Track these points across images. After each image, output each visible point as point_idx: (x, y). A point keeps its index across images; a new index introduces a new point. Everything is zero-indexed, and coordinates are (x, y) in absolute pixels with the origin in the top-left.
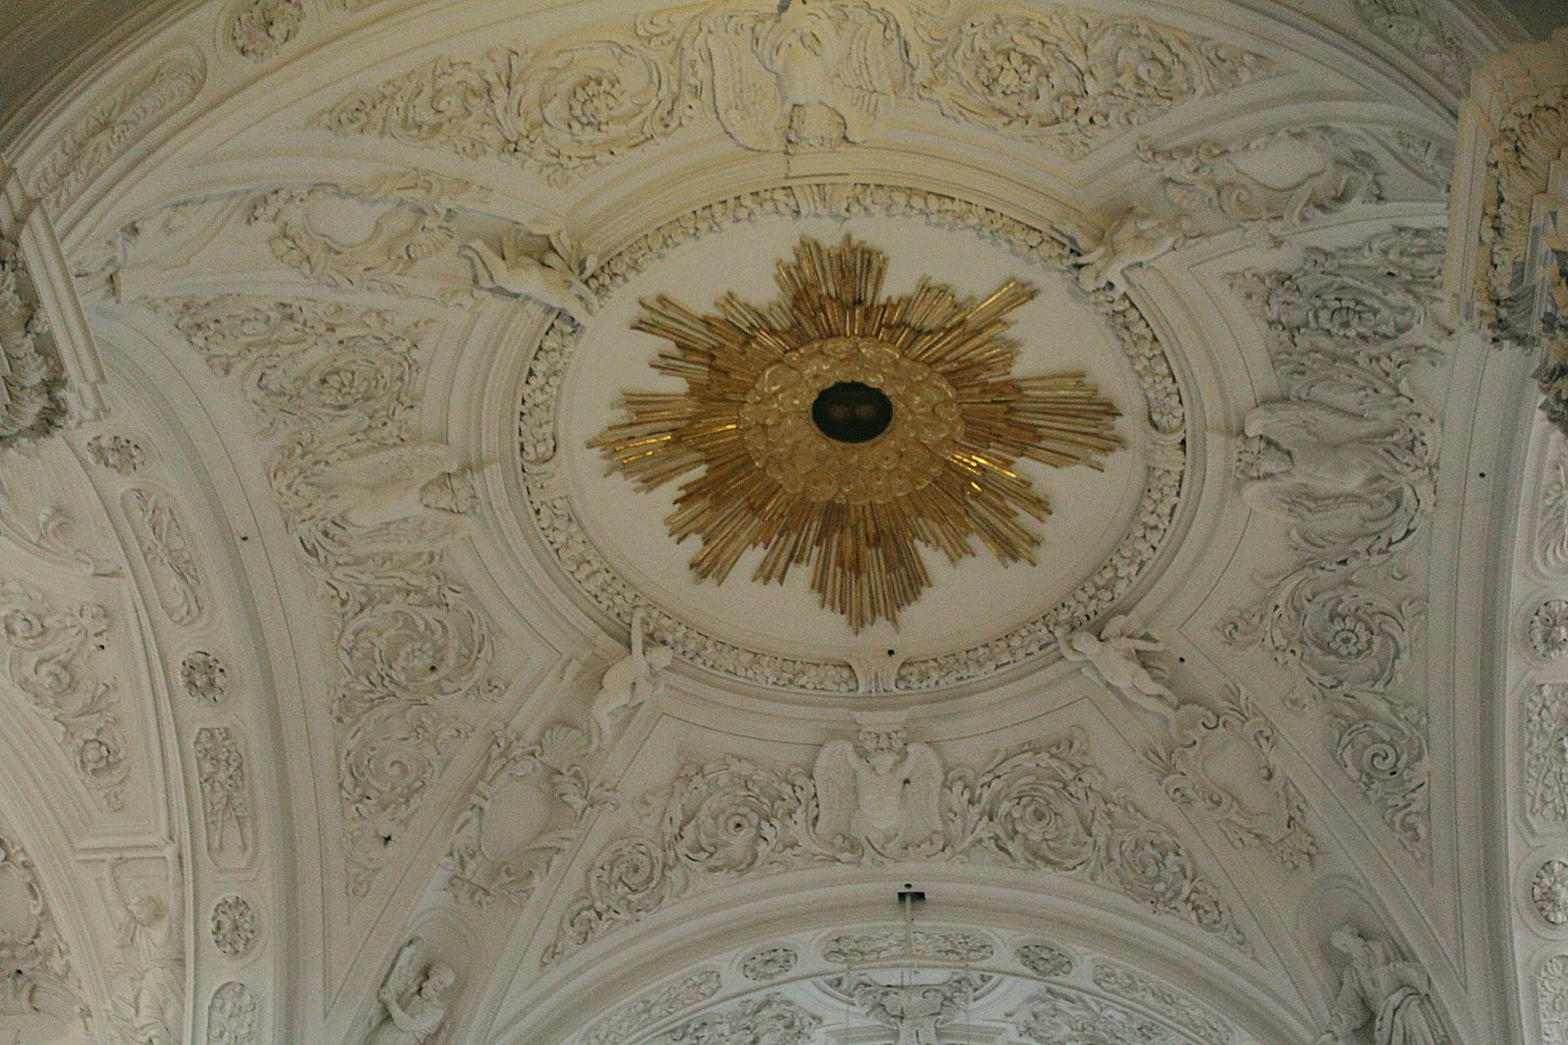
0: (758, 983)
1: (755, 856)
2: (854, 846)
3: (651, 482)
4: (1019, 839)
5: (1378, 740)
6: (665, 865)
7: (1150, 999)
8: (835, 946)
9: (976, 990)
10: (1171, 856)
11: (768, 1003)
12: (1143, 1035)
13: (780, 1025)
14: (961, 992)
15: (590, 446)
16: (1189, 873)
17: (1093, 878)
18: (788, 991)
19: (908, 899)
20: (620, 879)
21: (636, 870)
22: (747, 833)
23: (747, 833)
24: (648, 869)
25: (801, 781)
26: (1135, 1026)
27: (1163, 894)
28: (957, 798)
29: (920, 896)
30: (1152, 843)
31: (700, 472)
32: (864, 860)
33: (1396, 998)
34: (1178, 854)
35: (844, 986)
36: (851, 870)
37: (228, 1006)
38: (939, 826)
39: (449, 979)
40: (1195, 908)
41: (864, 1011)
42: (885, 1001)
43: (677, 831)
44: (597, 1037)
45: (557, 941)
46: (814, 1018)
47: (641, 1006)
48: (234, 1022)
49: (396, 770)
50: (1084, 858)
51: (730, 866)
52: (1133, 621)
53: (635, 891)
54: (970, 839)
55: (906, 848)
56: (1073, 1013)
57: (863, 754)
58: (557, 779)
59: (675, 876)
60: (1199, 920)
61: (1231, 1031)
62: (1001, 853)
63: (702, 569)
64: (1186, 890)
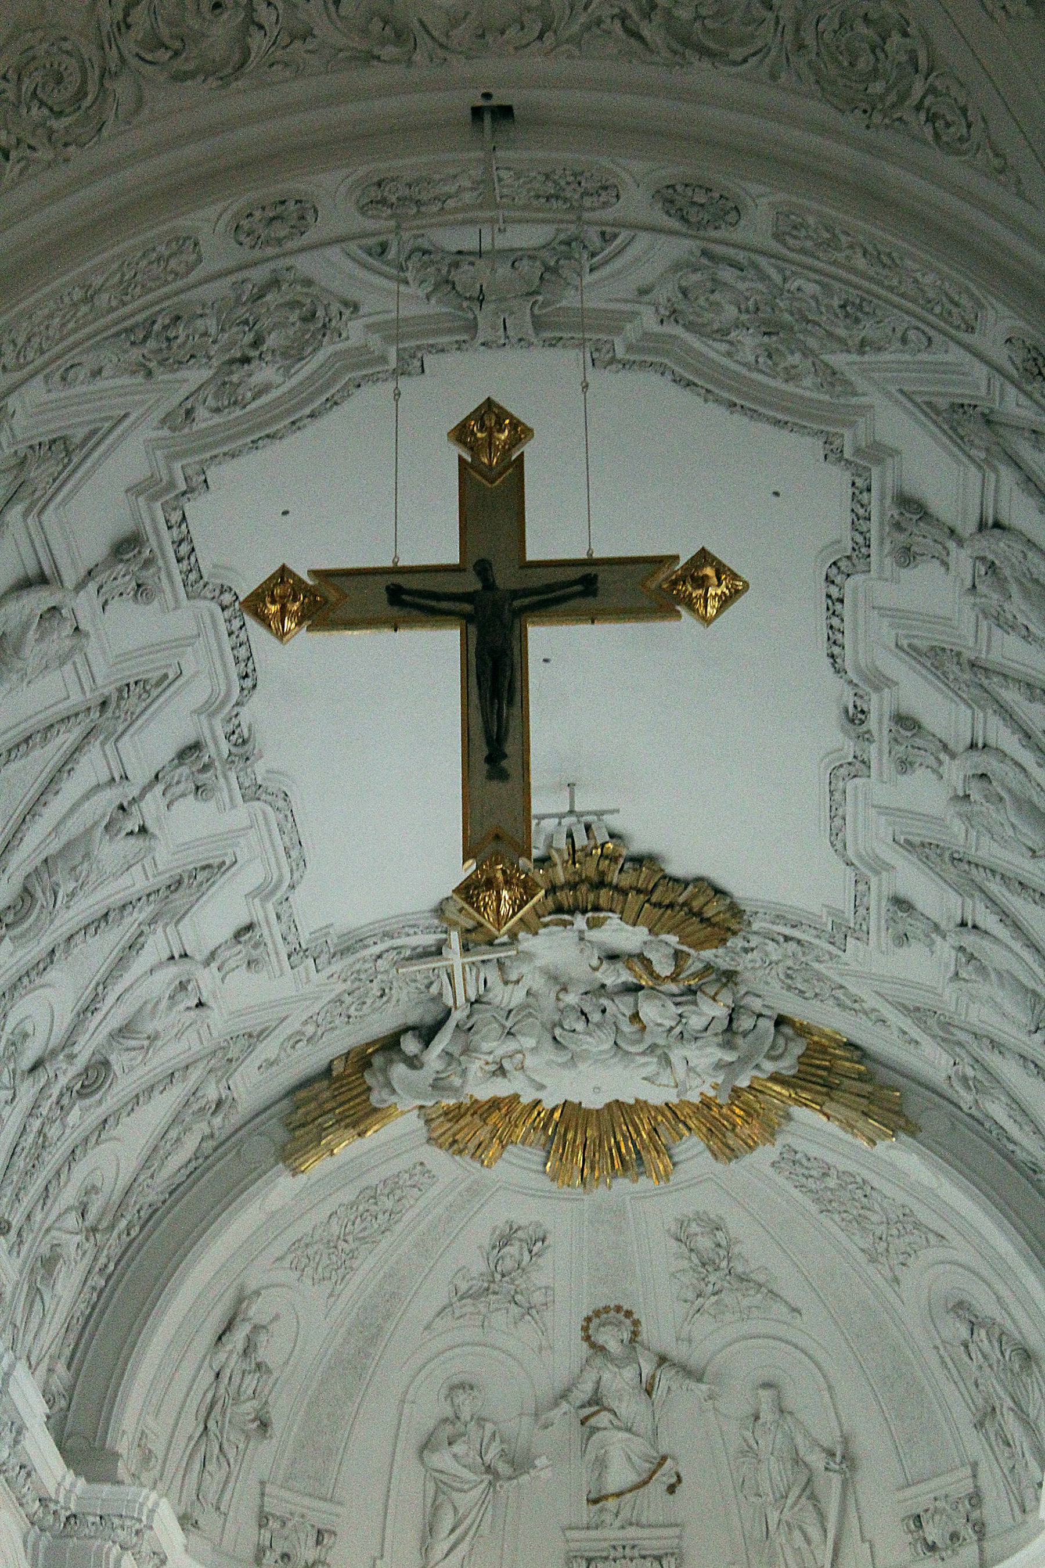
0: (257, 253)
1: (246, 53)
2: (400, 36)
4: (657, 17)
6: (104, 72)
7: (861, 263)
8: (374, 193)
9: (593, 255)
10: (896, 38)
11: (275, 283)
12: (847, 316)
13: (294, 316)
14: (569, 258)
17: (774, 77)
18: (305, 264)
19: (487, 118)
20: (34, 93)
21: (59, 80)
22: (230, 20)
24: (77, 78)
26: (836, 303)
27: (882, 98)
29: (505, 112)
32: (417, 57)
34: (905, 34)
35: (391, 254)
40: (932, 118)
41: (421, 293)
42: (456, 276)
43: (120, 16)
44: (14, 342)
46: (346, 304)
47: (78, 294)
50: (760, 44)
51: (204, 72)
53: (59, 114)
54: (583, 19)
55: (482, 36)
56: (742, 286)
59: (122, 88)
60: (937, 136)
61: (982, 307)
62: (632, 41)
64: (918, 88)
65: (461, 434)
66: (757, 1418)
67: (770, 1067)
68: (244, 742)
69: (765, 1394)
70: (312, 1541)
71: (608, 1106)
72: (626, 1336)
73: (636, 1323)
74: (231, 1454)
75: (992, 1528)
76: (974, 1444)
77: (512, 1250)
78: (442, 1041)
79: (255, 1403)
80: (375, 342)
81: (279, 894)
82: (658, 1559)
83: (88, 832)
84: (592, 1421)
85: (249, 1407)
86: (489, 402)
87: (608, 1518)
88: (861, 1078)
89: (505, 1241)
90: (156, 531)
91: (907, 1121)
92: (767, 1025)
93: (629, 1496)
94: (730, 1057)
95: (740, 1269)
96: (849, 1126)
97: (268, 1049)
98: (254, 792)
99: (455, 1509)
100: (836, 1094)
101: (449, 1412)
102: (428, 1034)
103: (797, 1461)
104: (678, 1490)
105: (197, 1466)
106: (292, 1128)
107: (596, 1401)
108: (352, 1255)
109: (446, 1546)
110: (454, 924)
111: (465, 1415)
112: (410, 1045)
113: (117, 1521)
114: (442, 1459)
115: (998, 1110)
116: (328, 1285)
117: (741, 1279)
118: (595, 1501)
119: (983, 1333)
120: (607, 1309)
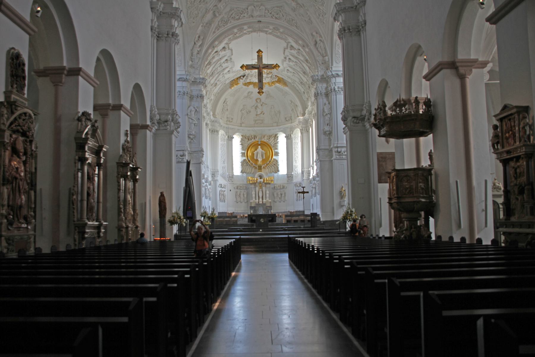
2: (252, 16)
5: (321, 12)
23: (239, 16)
25: (246, 10)
28: (267, 12)
29: (260, 21)
33: (319, 42)
38: (264, 14)
39: (202, 38)
51: (237, 19)
57: (254, 7)
59: (229, 22)
65: (257, 52)
66: (271, 108)
67: (275, 80)
69: (272, 106)
72: (260, 100)
77: (250, 93)
78: (245, 77)
80: (247, 32)
85: (226, 109)
88: (283, 81)
89: (249, 93)
92: (274, 76)
97: (229, 79)
98: (231, 62)
102: (244, 76)
103: (275, 112)
106: (231, 85)
107: (257, 106)
112: (242, 77)
114: (243, 112)
115: (295, 85)
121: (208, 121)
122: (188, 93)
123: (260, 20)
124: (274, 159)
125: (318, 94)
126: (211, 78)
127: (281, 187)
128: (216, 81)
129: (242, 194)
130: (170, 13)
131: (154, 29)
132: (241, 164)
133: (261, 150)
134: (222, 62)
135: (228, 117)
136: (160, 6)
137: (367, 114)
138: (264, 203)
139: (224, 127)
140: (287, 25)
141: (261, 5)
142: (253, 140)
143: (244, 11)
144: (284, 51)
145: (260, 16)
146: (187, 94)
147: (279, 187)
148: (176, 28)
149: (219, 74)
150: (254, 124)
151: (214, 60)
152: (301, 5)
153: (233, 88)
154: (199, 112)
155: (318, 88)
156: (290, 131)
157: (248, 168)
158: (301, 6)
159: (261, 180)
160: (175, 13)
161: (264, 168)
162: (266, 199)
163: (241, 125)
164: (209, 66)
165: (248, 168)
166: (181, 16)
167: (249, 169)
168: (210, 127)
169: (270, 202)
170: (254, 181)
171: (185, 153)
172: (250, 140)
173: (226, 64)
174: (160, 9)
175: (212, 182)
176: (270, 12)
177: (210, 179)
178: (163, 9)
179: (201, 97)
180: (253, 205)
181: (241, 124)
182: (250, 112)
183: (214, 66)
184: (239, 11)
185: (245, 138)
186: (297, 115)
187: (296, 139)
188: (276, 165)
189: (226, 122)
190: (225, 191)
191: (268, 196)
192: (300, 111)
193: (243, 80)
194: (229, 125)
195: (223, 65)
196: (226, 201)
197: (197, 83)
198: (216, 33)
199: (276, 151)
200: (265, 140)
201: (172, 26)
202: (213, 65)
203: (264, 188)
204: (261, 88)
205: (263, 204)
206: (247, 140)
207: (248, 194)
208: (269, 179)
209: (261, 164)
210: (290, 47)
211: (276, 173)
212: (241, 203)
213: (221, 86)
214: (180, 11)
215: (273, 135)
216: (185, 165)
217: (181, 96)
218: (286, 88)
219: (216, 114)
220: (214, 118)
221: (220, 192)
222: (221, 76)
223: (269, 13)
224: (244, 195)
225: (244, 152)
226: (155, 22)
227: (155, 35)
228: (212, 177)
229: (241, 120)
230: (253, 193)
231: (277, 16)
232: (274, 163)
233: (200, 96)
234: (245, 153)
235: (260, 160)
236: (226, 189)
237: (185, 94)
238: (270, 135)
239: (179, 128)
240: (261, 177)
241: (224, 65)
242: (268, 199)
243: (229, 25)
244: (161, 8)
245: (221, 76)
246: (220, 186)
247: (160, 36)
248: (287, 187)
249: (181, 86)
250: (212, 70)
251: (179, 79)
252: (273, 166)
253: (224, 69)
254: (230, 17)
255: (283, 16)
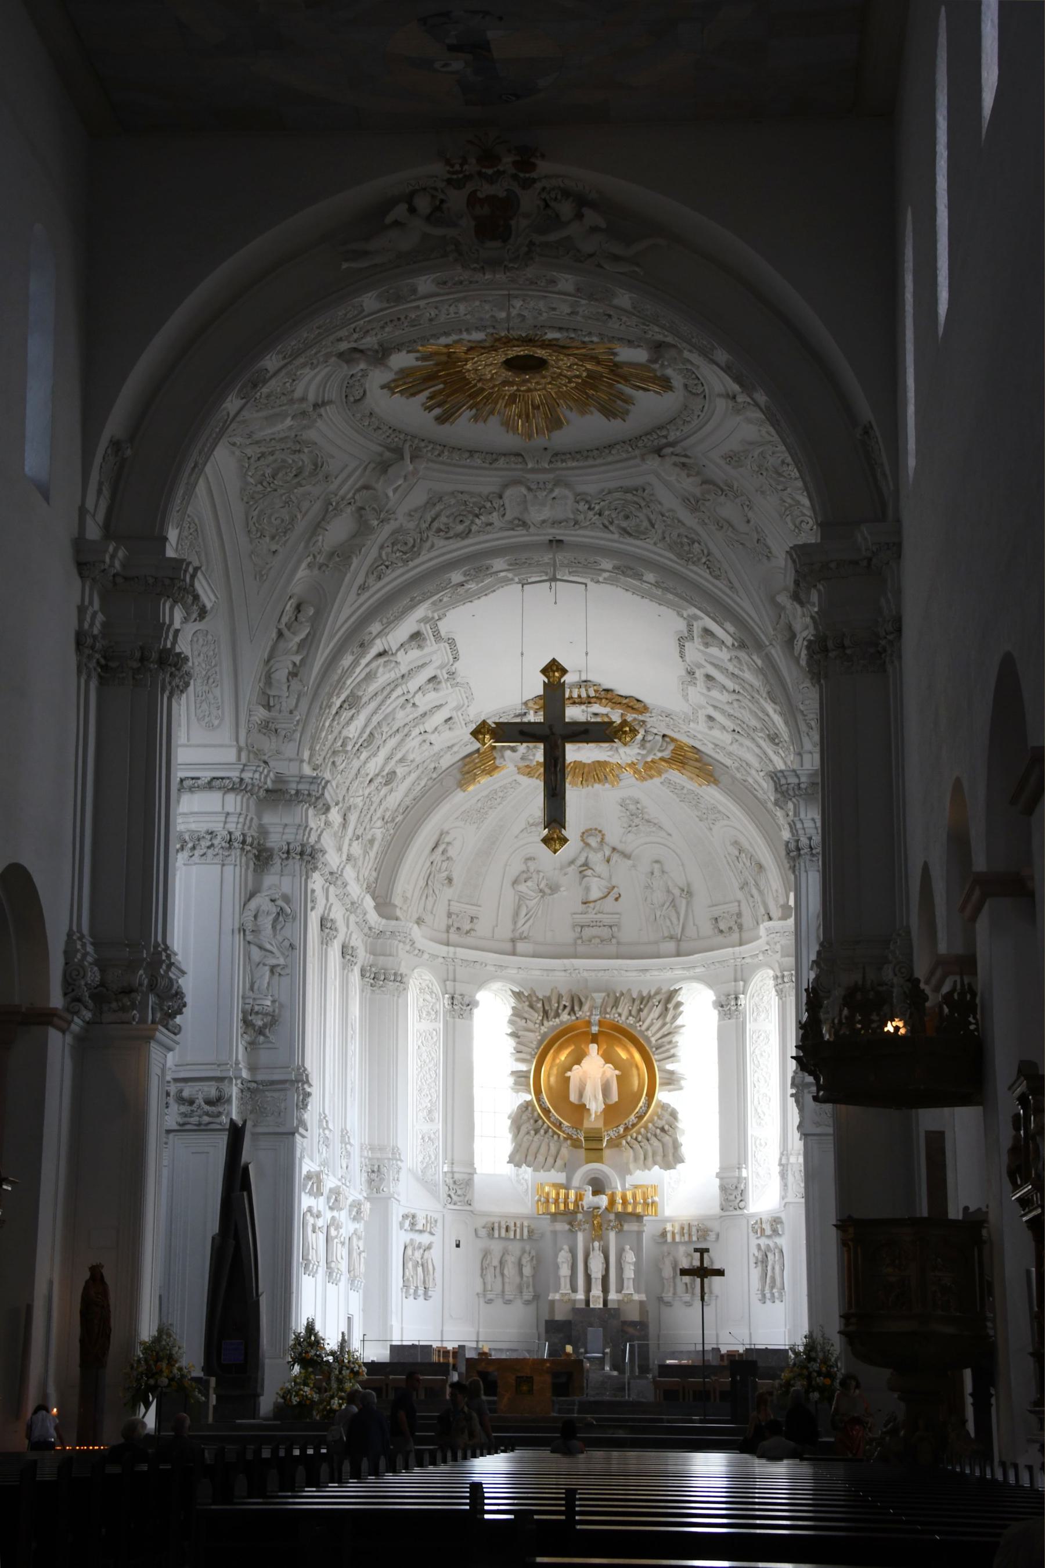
2: (524, 524)
3: (413, 395)
15: (383, 387)
16: (706, 552)
19: (554, 543)
23: (467, 523)
30: (686, 536)
31: (441, 386)
36: (524, 532)
37: (201, 640)
39: (311, 611)
45: (365, 582)
48: (205, 649)
49: (279, 521)
52: (678, 449)
57: (529, 489)
58: (363, 512)
59: (428, 544)
63: (441, 420)
65: (544, 671)
66: (652, 873)
67: (660, 755)
68: (453, 673)
69: (656, 866)
70: (469, 922)
71: (593, 762)
72: (599, 840)
73: (603, 835)
74: (437, 893)
75: (745, 927)
76: (740, 895)
79: (446, 873)
81: (463, 709)
82: (611, 927)
83: (395, 709)
84: (585, 873)
85: (445, 874)
86: (554, 661)
87: (590, 910)
88: (697, 760)
90: (426, 630)
91: (715, 780)
93: (599, 902)
94: (644, 752)
95: (646, 817)
96: (692, 779)
97: (455, 749)
99: (527, 907)
100: (686, 766)
101: (524, 868)
103: (669, 891)
104: (620, 900)
105: (424, 898)
107: (586, 864)
108: (486, 813)
109: (523, 921)
110: (532, 708)
111: (532, 869)
113: (397, 934)
114: (522, 888)
116: (476, 825)
117: (648, 821)
118: (585, 903)
119: (744, 855)
120: (591, 829)
121: (354, 936)
122: (249, 840)
123: (559, 538)
124: (664, 1107)
125: (798, 849)
126: (364, 755)
127: (690, 1235)
128: (393, 762)
129: (511, 1260)
130: (151, 581)
131: (89, 641)
132: (509, 1122)
133: (602, 1061)
134: (412, 690)
135: (453, 909)
136: (113, 557)
137: (895, 980)
138: (610, 1306)
139: (434, 956)
140: (671, 560)
141: (557, 483)
142: (565, 1017)
143: (488, 505)
144: (682, 647)
145: (557, 523)
146: (244, 842)
147: (683, 1235)
148: (177, 631)
149: (403, 732)
150: (575, 944)
151: (373, 687)
152: (721, 485)
153: (471, 788)
154: (294, 918)
155: (799, 826)
156: (736, 981)
157: (541, 1142)
158: (722, 490)
159: (596, 1199)
160: (172, 579)
161: (614, 1144)
162: (620, 1290)
163: (514, 947)
164: (353, 711)
165: (541, 1142)
166: (197, 584)
167: (543, 1149)
168: (362, 956)
169: (641, 1303)
170: (566, 1204)
171: (226, 1090)
172: (552, 1014)
173: (432, 695)
174: (112, 565)
175: (367, 1206)
176: (597, 507)
177: (356, 1191)
178: (124, 566)
179: (302, 854)
180: (559, 1316)
181: (513, 941)
182: (554, 888)
183: (378, 708)
184: (465, 503)
185: (531, 1006)
186: (762, 911)
187: (763, 1016)
188: (670, 1133)
189: (444, 936)
190: (429, 1248)
191: (629, 1273)
192: (777, 891)
193: (518, 755)
194: (455, 946)
195: (418, 699)
196: (435, 1293)
197: (288, 797)
198: (374, 589)
199: (670, 1067)
200: (622, 1015)
201: (160, 628)
202: (373, 705)
203: (612, 1236)
204: (555, 821)
205: (608, 1315)
206: (537, 1017)
207: (538, 1262)
208: (634, 1197)
209: (600, 1124)
210: (702, 637)
211: (668, 1166)
212: (508, 1302)
213: (419, 778)
214: (191, 570)
215: (657, 993)
216: (221, 1142)
217: (221, 851)
218: (712, 794)
219: (397, 900)
220: (384, 921)
221: (409, 1251)
222: (413, 742)
223: (591, 513)
224: (520, 1266)
225: (522, 1067)
226: (94, 615)
227: (92, 664)
228: (370, 1181)
229: (515, 923)
230: (560, 1260)
231: (624, 524)
232: (660, 1123)
233: (299, 849)
234: (529, 1072)
235: (595, 1105)
236: (436, 1240)
237: (236, 844)
238: (645, 994)
239: (181, 1013)
240: (598, 1187)
241: (424, 702)
242: (629, 1289)
243: (425, 561)
244: (117, 564)
245: (416, 742)
246: (407, 1223)
247: (113, 664)
248: (718, 1235)
249: (220, 809)
250: (366, 726)
251: (210, 783)
252: (655, 1136)
253: (424, 715)
254: (429, 528)
255: (653, 526)
